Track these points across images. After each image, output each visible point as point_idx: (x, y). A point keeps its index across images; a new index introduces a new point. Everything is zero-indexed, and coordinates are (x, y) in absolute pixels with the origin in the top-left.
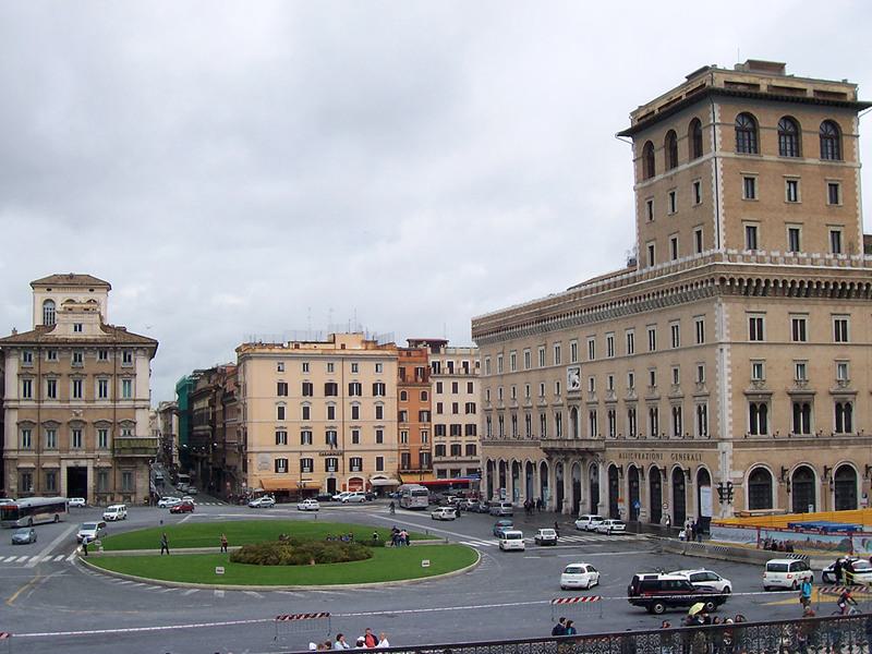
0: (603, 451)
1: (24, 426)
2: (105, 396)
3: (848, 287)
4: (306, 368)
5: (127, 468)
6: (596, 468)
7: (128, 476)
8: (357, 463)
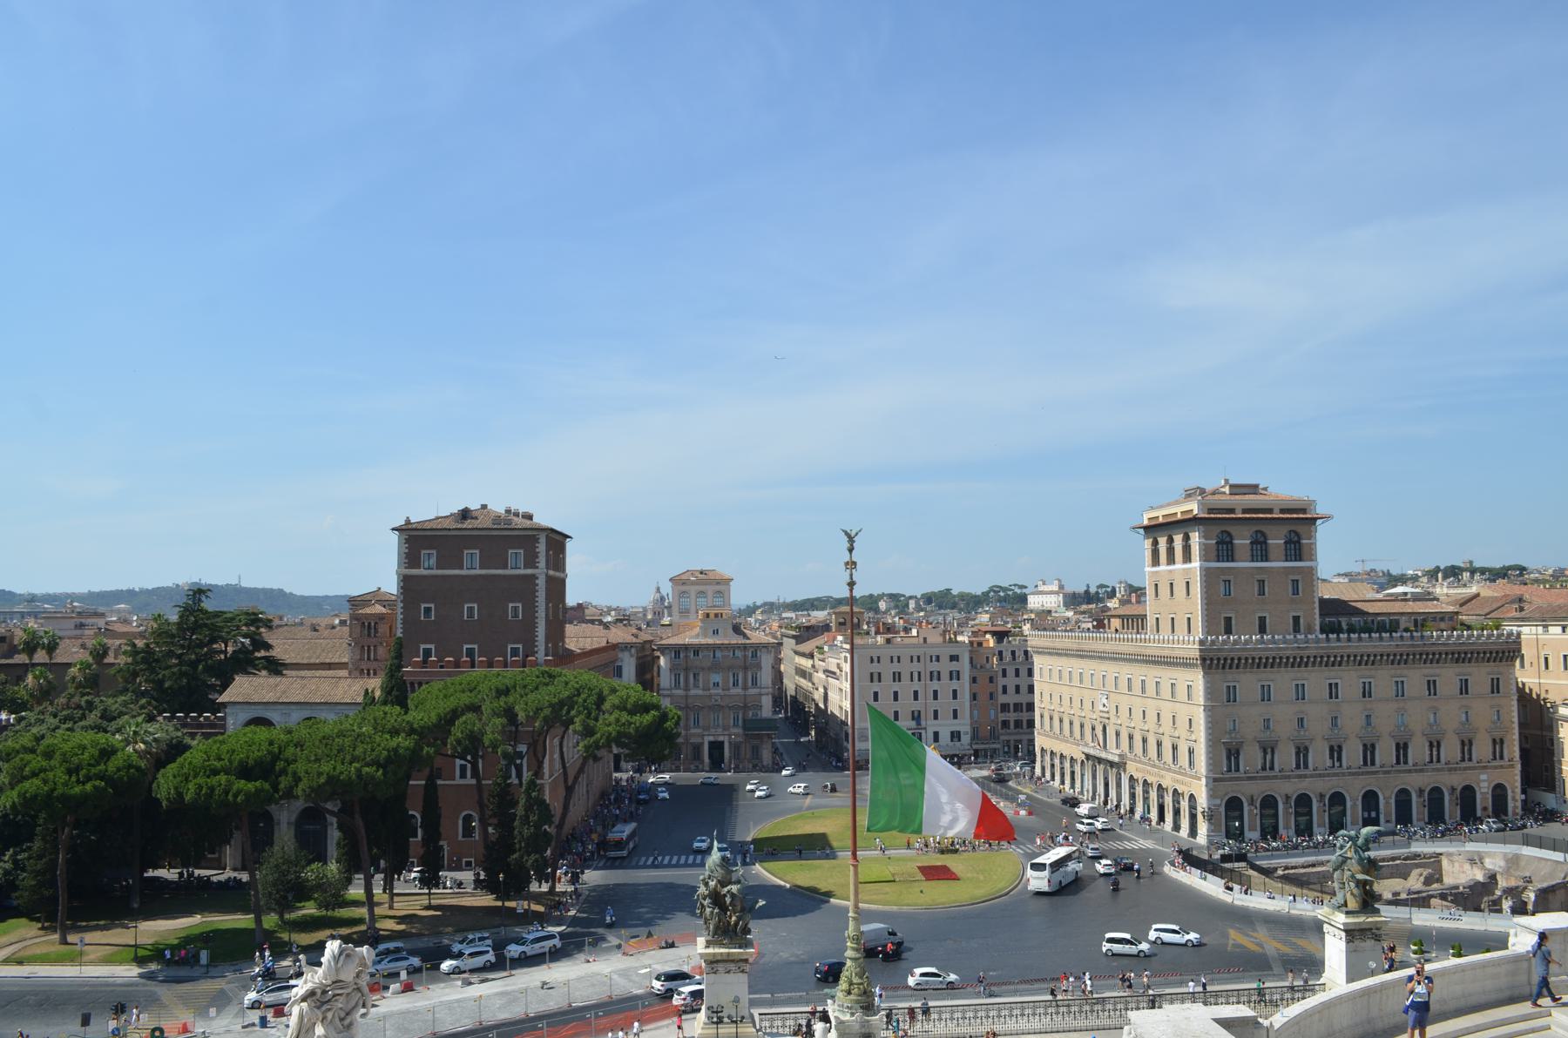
5: (756, 742)
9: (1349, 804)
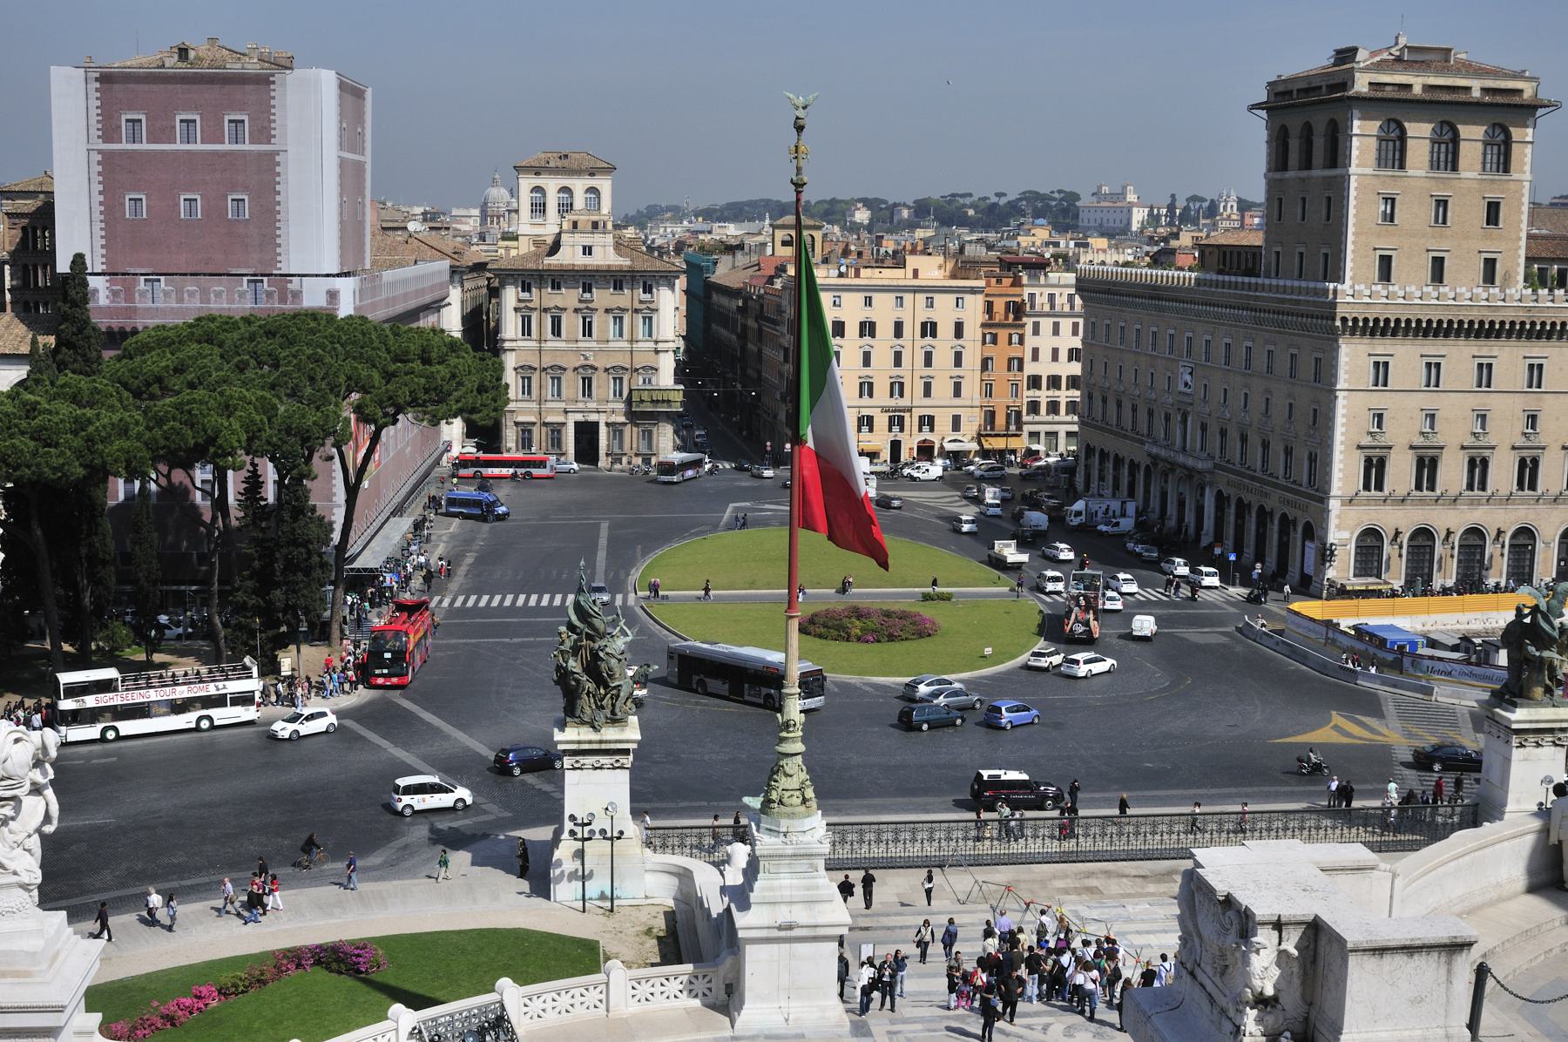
0: (1209, 472)
1: (525, 371)
2: (621, 335)
4: (868, 302)
6: (1203, 489)
7: (648, 435)
8: (928, 422)
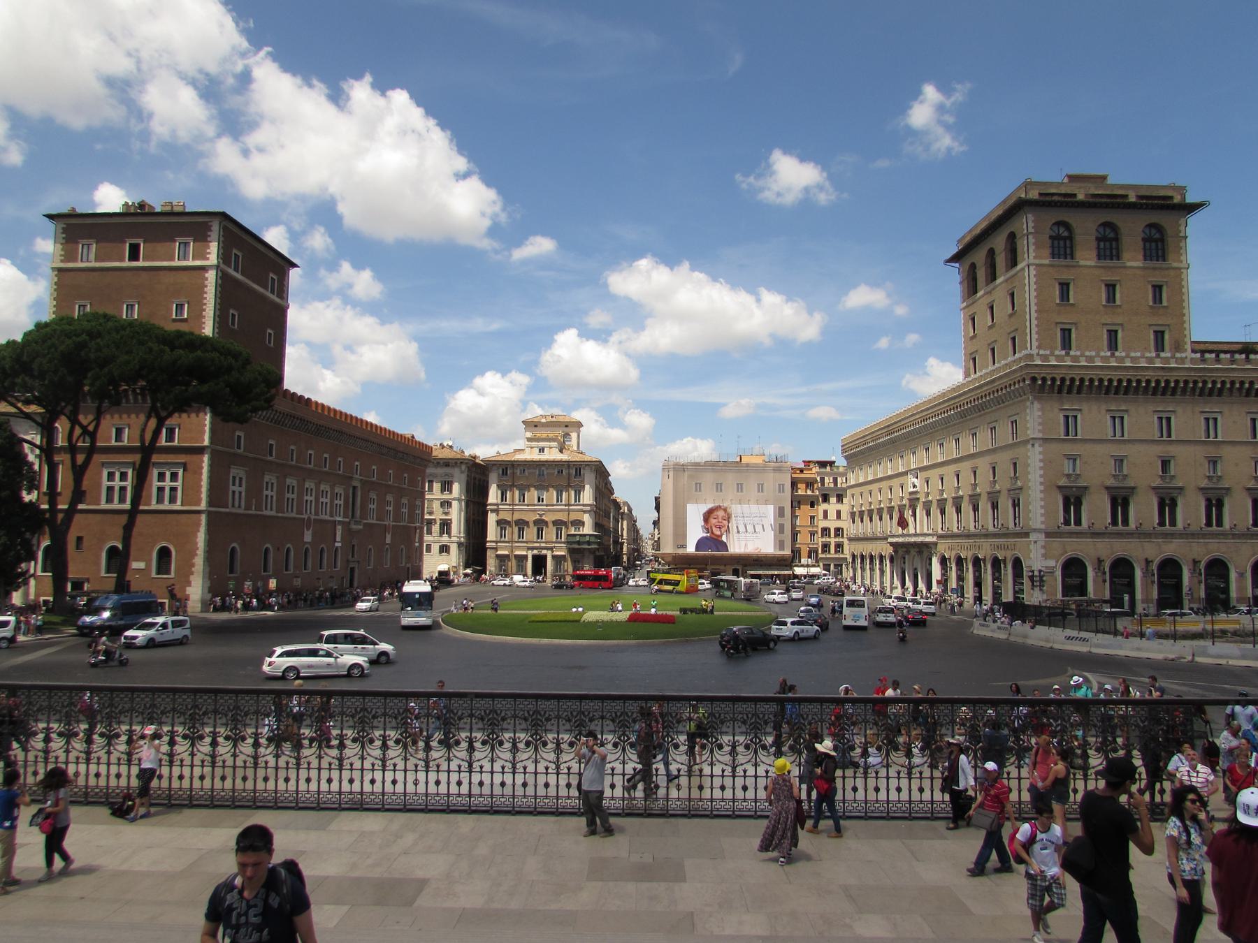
0: (936, 544)
3: (1172, 384)
5: (577, 556)
9: (1233, 576)
